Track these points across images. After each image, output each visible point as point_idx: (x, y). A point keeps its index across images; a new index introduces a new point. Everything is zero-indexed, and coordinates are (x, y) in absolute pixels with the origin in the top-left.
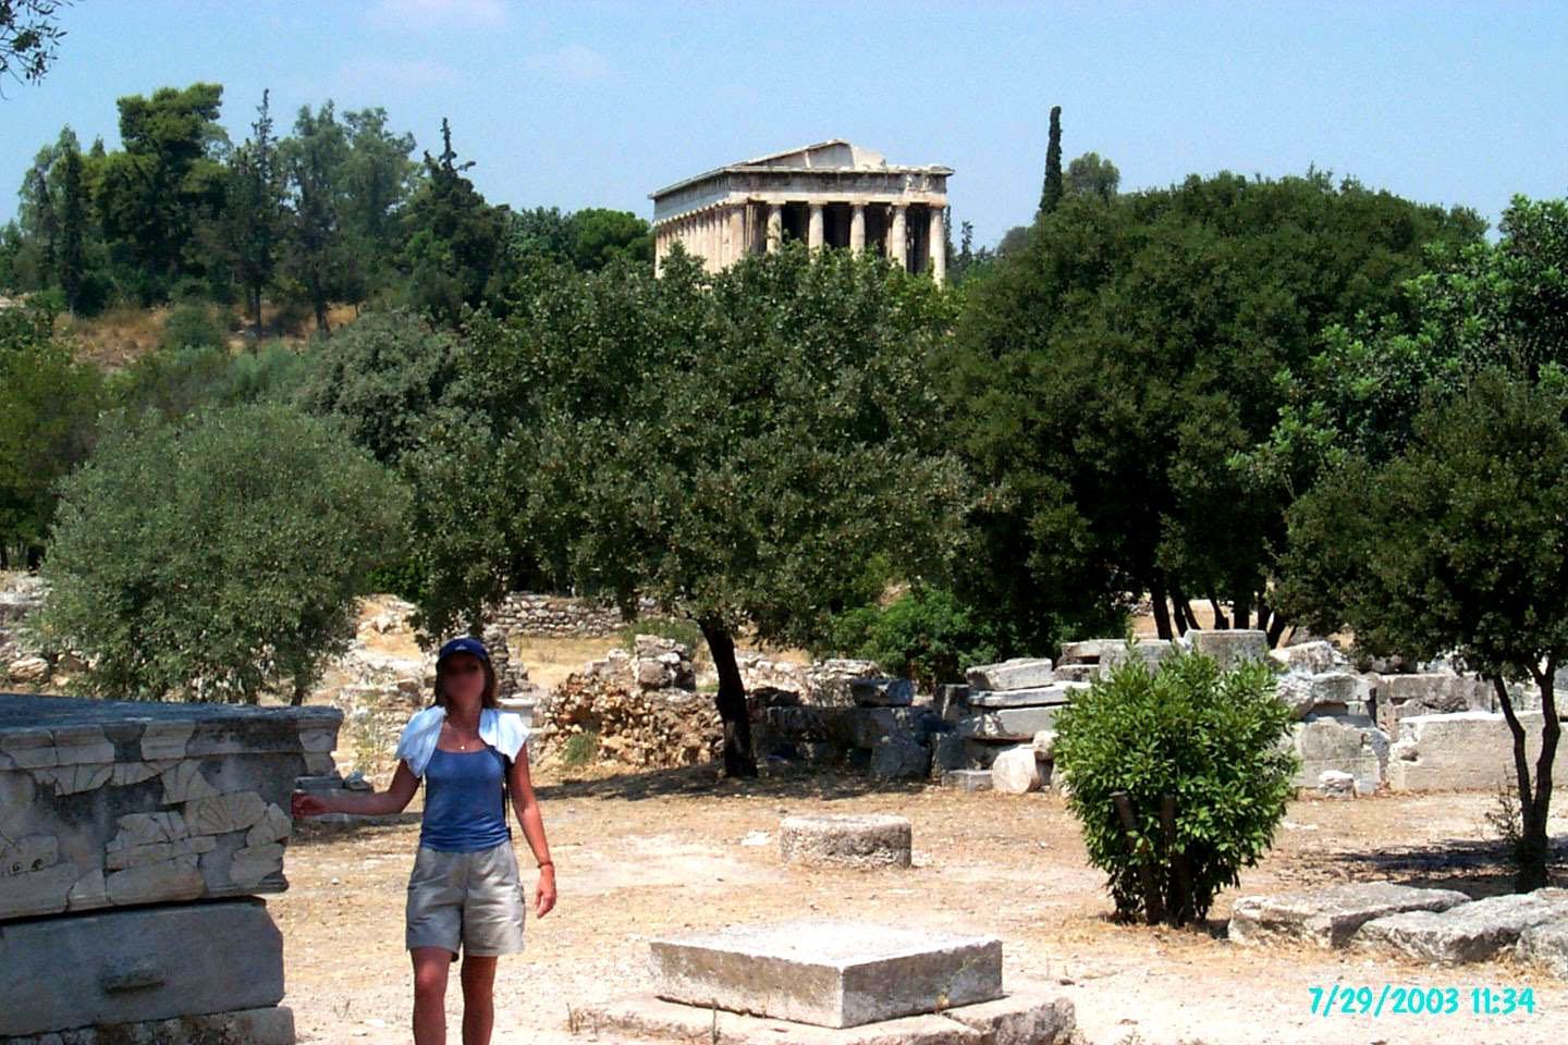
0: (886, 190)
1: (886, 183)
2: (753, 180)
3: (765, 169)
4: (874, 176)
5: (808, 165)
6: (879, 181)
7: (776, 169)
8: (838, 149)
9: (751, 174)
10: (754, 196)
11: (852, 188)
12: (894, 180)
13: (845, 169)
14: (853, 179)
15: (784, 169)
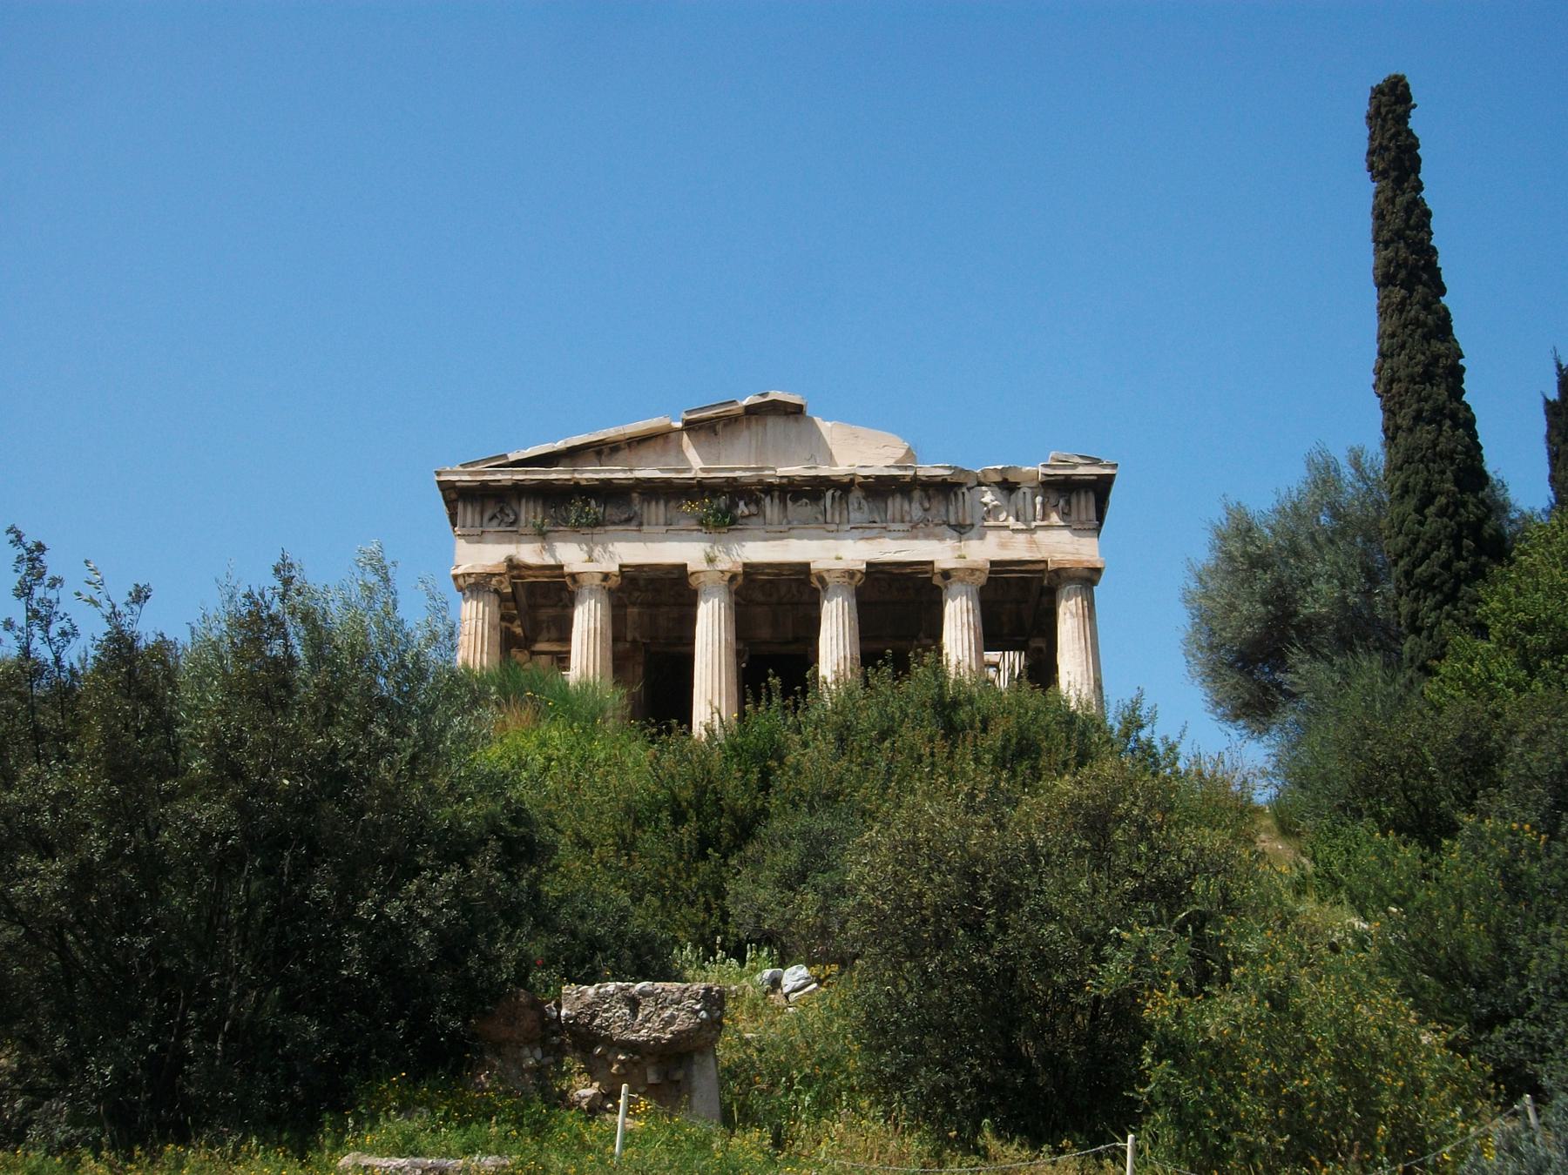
0: (915, 530)
1: (916, 512)
2: (529, 513)
3: (557, 474)
4: (880, 489)
5: (695, 462)
6: (895, 505)
7: (590, 473)
8: (774, 425)
9: (519, 491)
10: (529, 553)
11: (825, 527)
12: (934, 496)
13: (796, 470)
14: (816, 497)
15: (614, 472)
